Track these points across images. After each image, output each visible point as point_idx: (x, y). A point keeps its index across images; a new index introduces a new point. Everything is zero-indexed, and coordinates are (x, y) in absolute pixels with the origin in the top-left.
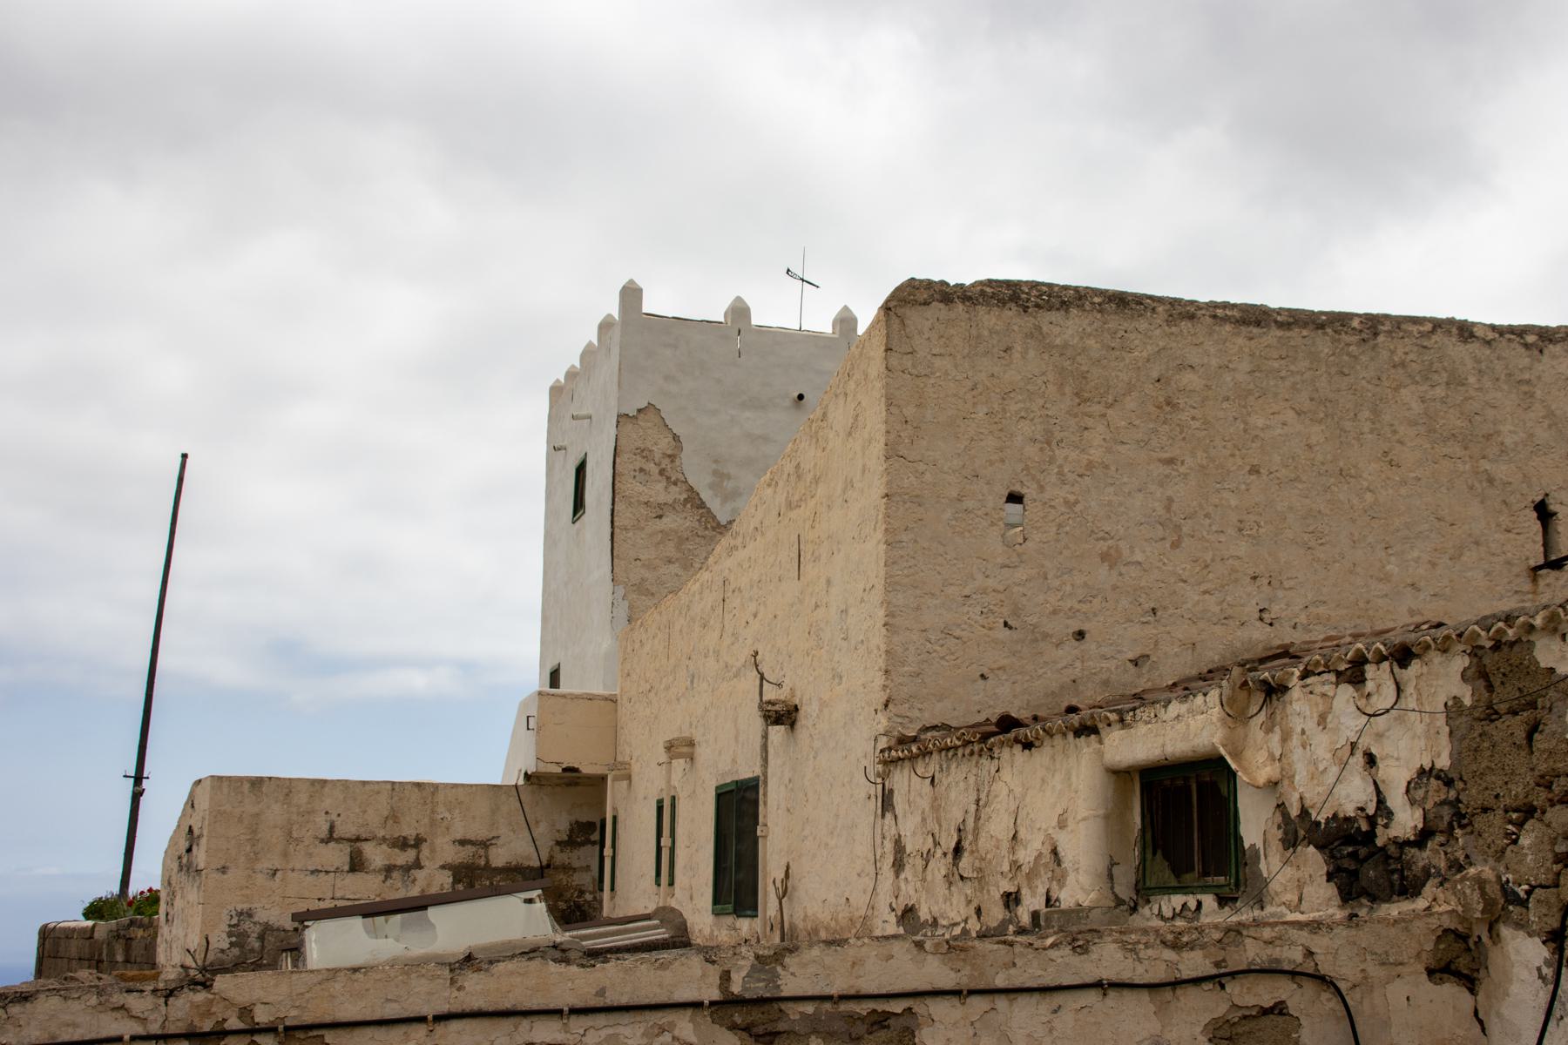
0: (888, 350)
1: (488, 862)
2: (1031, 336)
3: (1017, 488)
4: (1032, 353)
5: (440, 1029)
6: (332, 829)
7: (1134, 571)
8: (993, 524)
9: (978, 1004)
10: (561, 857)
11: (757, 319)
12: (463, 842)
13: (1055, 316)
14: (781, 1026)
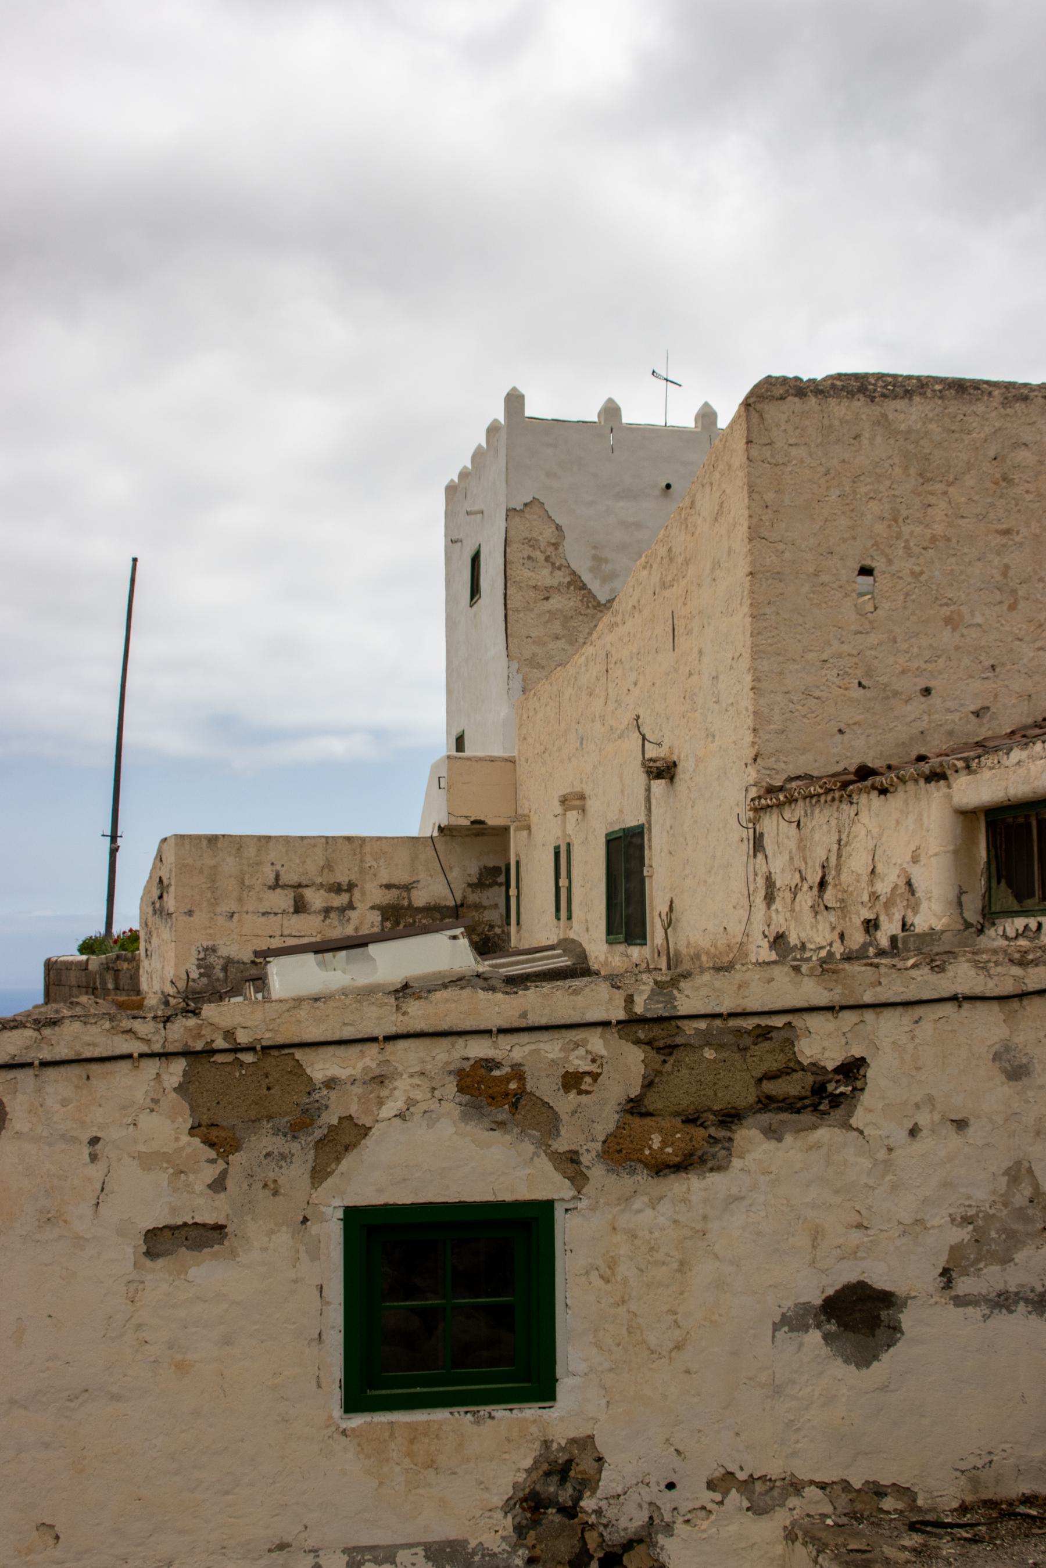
0: (749, 442)
1: (410, 903)
2: (879, 423)
3: (868, 562)
4: (879, 440)
5: (390, 1047)
6: (277, 877)
7: (974, 633)
8: (846, 595)
9: (849, 1018)
10: (473, 897)
11: (627, 418)
12: (388, 887)
13: (901, 404)
14: (679, 1040)
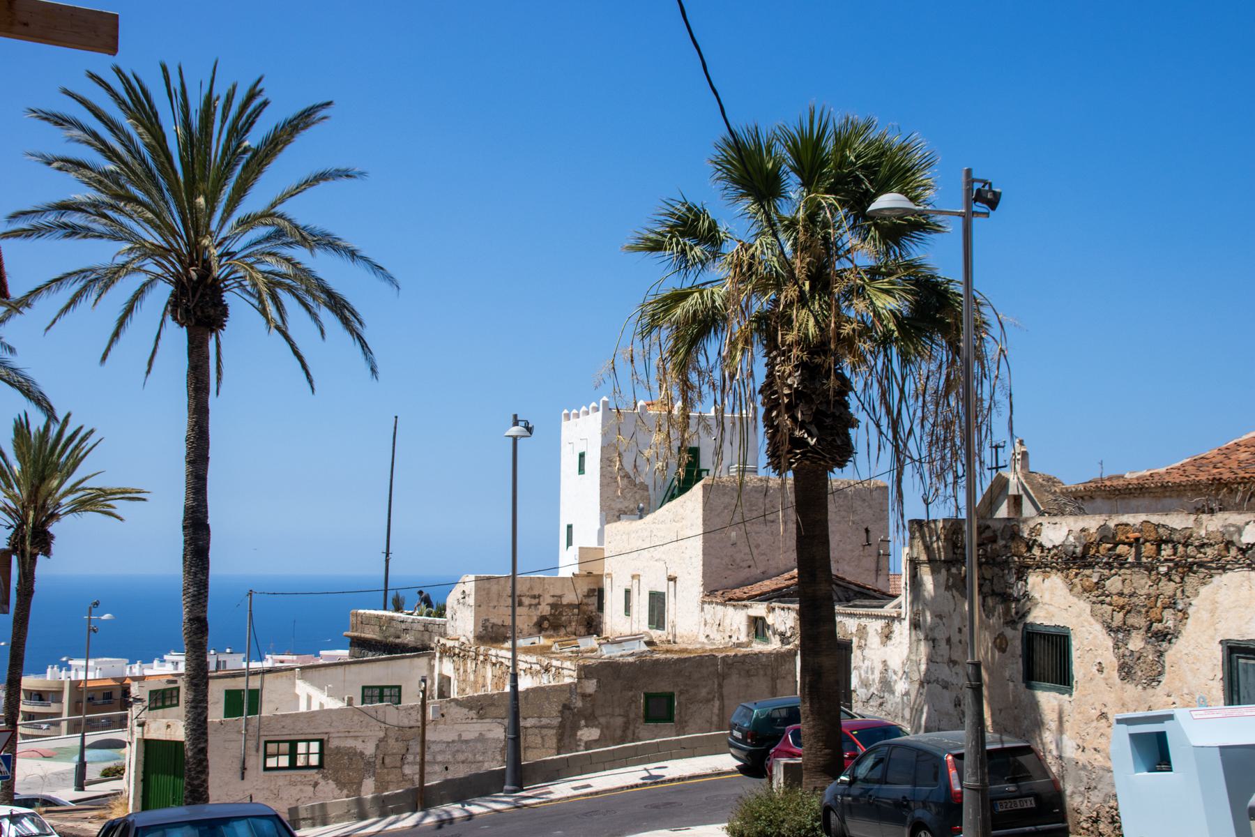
10: (585, 601)
